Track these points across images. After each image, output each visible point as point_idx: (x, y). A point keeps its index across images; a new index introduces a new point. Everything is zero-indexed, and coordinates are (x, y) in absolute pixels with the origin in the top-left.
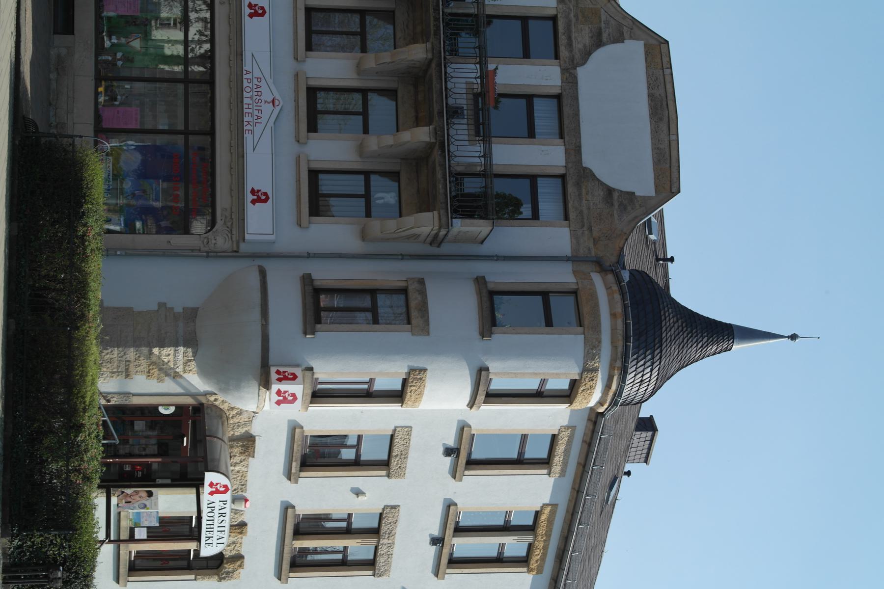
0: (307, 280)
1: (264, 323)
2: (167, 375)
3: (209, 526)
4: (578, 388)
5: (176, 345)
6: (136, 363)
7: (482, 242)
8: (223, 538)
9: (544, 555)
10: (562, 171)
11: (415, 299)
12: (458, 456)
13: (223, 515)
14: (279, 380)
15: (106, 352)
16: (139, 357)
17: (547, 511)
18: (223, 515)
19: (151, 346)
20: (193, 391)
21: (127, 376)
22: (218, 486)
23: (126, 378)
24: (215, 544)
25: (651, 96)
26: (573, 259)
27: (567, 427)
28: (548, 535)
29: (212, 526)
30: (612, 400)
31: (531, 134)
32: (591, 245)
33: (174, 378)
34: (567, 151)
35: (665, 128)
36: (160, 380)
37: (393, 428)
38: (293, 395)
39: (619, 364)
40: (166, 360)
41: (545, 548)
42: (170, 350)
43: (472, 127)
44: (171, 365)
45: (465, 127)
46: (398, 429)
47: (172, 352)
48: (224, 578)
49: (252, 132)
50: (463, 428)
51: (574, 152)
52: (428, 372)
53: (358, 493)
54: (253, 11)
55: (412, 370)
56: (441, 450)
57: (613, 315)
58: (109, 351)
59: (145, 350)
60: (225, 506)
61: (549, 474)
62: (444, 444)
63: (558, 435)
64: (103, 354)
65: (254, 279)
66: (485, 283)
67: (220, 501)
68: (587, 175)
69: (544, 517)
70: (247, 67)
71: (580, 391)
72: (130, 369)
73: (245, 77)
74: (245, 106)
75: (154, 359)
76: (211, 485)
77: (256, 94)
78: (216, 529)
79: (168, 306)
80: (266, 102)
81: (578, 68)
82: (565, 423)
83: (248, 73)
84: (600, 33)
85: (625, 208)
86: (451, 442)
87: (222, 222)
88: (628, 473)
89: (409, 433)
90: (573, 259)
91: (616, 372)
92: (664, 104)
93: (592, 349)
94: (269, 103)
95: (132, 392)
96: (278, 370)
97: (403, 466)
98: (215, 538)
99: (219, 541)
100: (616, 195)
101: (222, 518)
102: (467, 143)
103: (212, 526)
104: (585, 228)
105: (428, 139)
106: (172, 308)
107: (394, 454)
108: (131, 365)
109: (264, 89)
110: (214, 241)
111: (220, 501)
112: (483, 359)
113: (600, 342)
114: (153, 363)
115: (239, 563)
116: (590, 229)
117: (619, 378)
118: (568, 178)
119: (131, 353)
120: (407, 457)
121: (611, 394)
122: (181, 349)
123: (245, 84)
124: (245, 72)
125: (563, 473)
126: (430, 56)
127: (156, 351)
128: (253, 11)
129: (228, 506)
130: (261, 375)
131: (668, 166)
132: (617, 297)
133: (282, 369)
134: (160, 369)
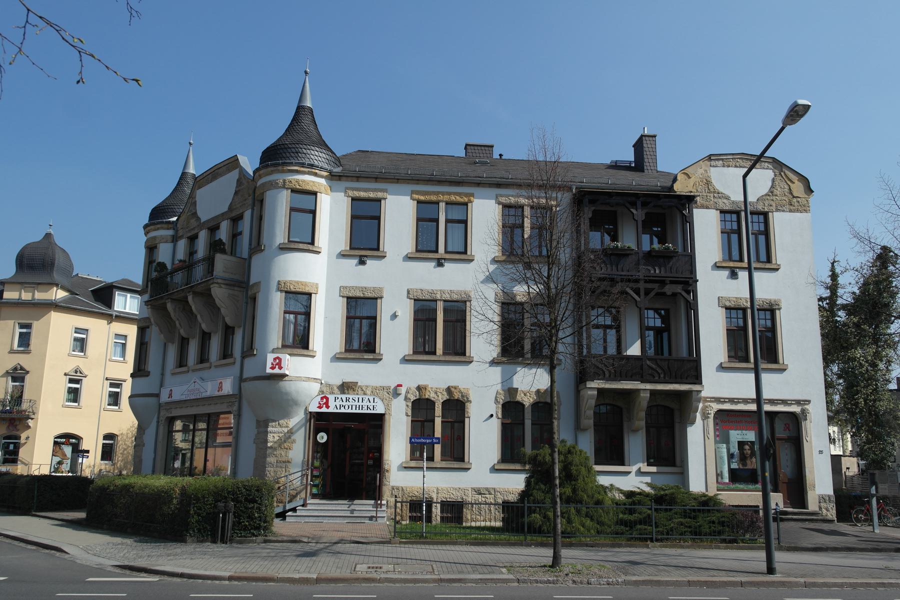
2: (290, 437)
4: (298, 189)
5: (267, 432)
6: (280, 457)
8: (341, 398)
9: (455, 194)
12: (366, 256)
13: (348, 399)
15: (268, 475)
16: (274, 455)
17: (416, 196)
18: (348, 399)
19: (267, 448)
20: (304, 421)
21: (289, 462)
23: (290, 462)
24: (374, 404)
27: (346, 192)
28: (437, 193)
29: (358, 406)
30: (308, 168)
33: (292, 433)
35: (220, 170)
36: (294, 441)
37: (341, 298)
38: (275, 359)
39: (280, 168)
40: (278, 438)
41: (449, 194)
42: (270, 438)
44: (281, 435)
46: (342, 295)
47: (272, 435)
48: (467, 398)
50: (343, 255)
52: (281, 279)
53: (394, 316)
55: (279, 289)
56: (361, 267)
58: (268, 473)
59: (269, 451)
60: (340, 398)
61: (385, 199)
62: (727, 278)
63: (352, 197)
64: (270, 476)
67: (335, 401)
68: (231, 208)
69: (422, 198)
71: (301, 188)
72: (284, 460)
75: (276, 445)
76: (320, 407)
78: (360, 403)
82: (343, 194)
83: (186, 398)
86: (726, 273)
88: (501, 155)
89: (346, 287)
91: (285, 168)
93: (273, 185)
95: (302, 459)
96: (280, 370)
97: (372, 289)
98: (368, 404)
99: (372, 400)
103: (358, 406)
104: (245, 202)
107: (362, 295)
108: (280, 459)
111: (335, 401)
112: (274, 247)
113: (270, 181)
114: (280, 446)
115: (453, 390)
117: (289, 166)
119: (271, 460)
120: (365, 287)
121: (302, 169)
122: (269, 429)
123: (188, 398)
125: (385, 191)
126: (169, 300)
127: (269, 445)
130: (274, 380)
134: (285, 442)
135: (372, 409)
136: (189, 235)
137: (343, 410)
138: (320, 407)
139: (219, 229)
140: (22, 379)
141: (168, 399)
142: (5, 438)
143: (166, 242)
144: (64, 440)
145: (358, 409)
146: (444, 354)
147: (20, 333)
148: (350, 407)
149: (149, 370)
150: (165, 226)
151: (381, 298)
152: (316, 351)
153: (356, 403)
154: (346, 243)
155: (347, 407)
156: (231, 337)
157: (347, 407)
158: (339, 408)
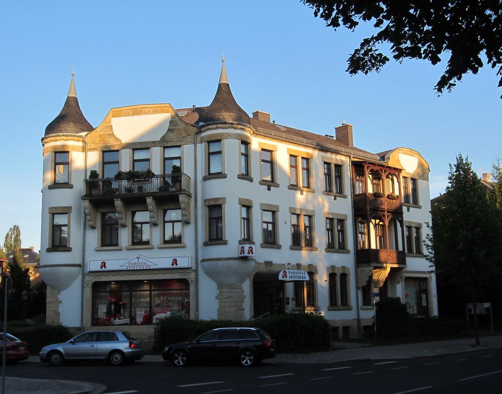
0: (206, 244)
1: (222, 259)
7: (190, 178)
10: (162, 148)
11: (212, 203)
14: (244, 253)
22: (284, 275)
25: (133, 115)
26: (195, 144)
31: (148, 160)
32: (190, 137)
34: (154, 146)
38: (249, 248)
43: (146, 182)
45: (146, 185)
49: (150, 266)
51: (154, 144)
54: (103, 267)
57: (217, 128)
65: (206, 264)
66: (205, 177)
68: (163, 139)
70: (125, 268)
73: (129, 269)
74: (140, 268)
77: (135, 265)
78: (299, 275)
79: (217, 295)
80: (138, 261)
81: (122, 143)
84: (109, 134)
85: (176, 124)
87: (185, 276)
90: (195, 144)
92: (135, 110)
94: (138, 260)
100: (171, 128)
102: (152, 185)
105: (151, 199)
106: (218, 294)
109: (133, 262)
110: (192, 279)
113: (227, 133)
116: (184, 137)
118: (165, 146)
123: (131, 269)
124: (127, 269)
128: (103, 267)
129: (291, 271)
131: (159, 108)
132: (210, 127)
133: (240, 252)
143: (78, 151)
146: (416, 254)
149: (71, 247)
151: (314, 216)
153: (298, 275)
156: (330, 241)
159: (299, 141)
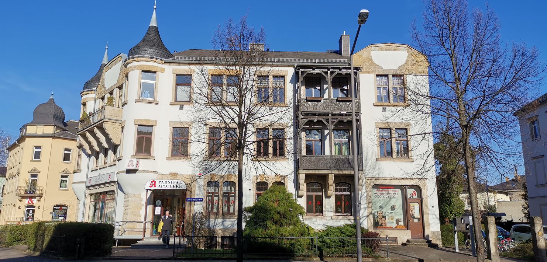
3: (173, 186)
13: (166, 182)
29: (171, 186)
39: (136, 59)
60: (162, 182)
99: (179, 183)
101: (168, 182)
103: (171, 186)
135: (179, 187)
136: (101, 96)
137: (163, 188)
138: (151, 187)
139: (113, 94)
140: (36, 176)
141: (89, 184)
142: (28, 207)
144: (59, 208)
145: (171, 187)
147: (35, 151)
148: (167, 186)
149: (81, 169)
150: (90, 92)
152: (155, 157)
154: (172, 99)
155: (165, 186)
157: (165, 186)
158: (161, 187)
159: (189, 60)
